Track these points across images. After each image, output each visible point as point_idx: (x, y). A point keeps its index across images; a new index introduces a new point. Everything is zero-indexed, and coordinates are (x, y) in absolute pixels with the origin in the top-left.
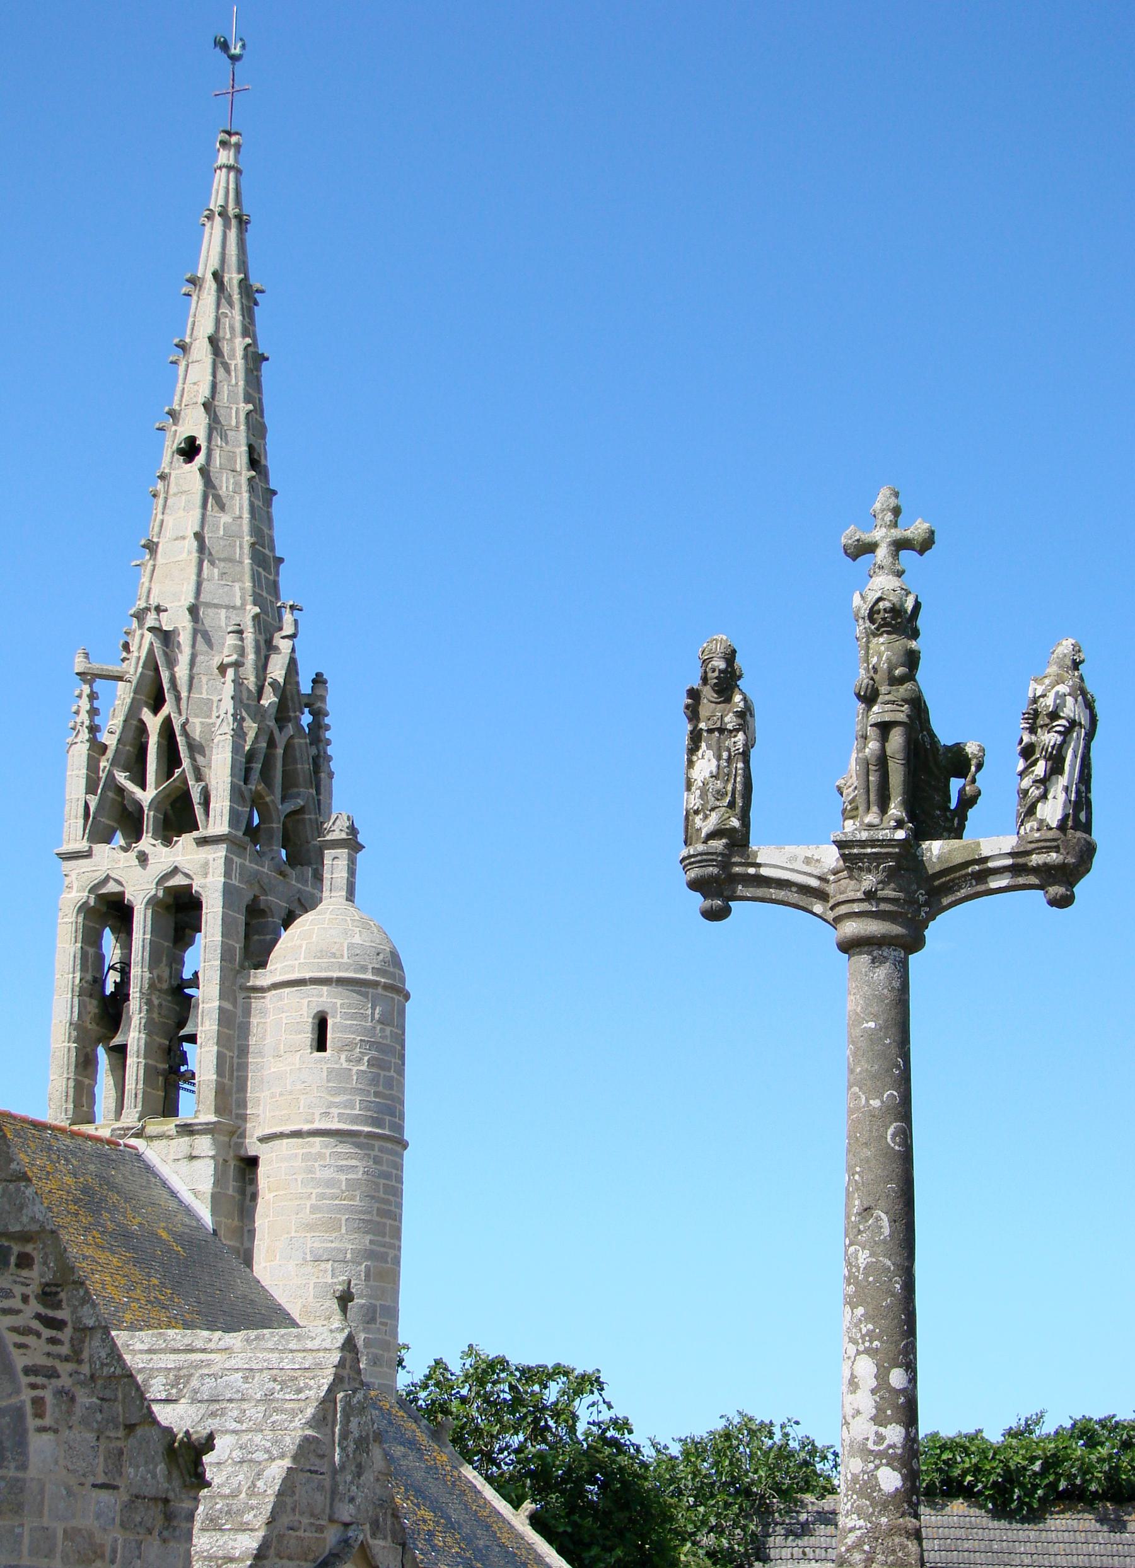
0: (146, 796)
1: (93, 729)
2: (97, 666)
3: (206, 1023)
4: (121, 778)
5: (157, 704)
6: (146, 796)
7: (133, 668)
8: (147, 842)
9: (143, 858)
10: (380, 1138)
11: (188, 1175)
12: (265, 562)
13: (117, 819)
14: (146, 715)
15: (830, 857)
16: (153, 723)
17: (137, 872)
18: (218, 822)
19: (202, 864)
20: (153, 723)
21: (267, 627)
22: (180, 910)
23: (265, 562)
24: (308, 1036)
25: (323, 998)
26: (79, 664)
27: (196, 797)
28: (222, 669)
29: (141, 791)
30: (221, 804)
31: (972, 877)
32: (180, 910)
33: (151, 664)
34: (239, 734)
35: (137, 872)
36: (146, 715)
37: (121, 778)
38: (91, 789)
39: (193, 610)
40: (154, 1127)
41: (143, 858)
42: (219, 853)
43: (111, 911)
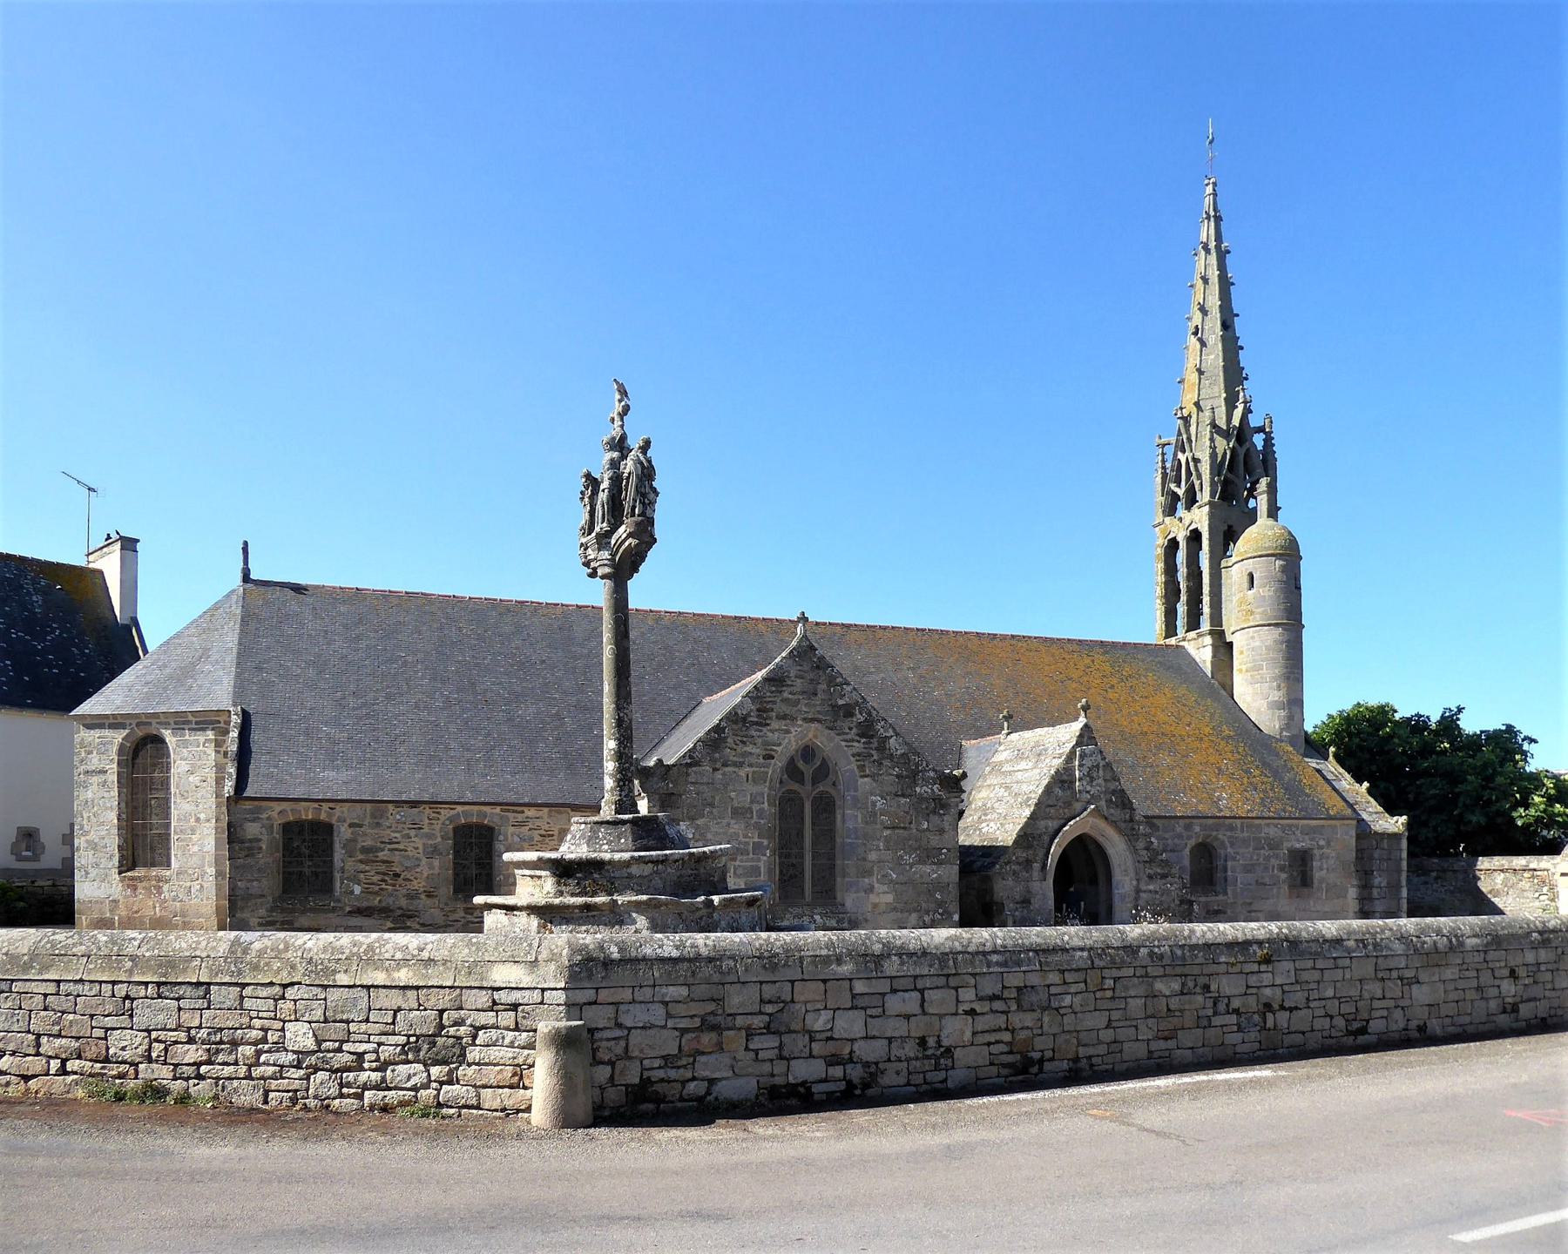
0: (1181, 492)
1: (1164, 468)
2: (1163, 441)
4: (1173, 486)
6: (1181, 492)
9: (1181, 519)
10: (1290, 620)
11: (1201, 651)
14: (1181, 456)
18: (1204, 496)
19: (1199, 518)
22: (1195, 536)
24: (1246, 585)
25: (1249, 565)
26: (1158, 441)
27: (1197, 488)
33: (1179, 434)
34: (1213, 455)
36: (1181, 456)
39: (1197, 404)
40: (1192, 634)
41: (1181, 519)
42: (1207, 508)
43: (1173, 545)
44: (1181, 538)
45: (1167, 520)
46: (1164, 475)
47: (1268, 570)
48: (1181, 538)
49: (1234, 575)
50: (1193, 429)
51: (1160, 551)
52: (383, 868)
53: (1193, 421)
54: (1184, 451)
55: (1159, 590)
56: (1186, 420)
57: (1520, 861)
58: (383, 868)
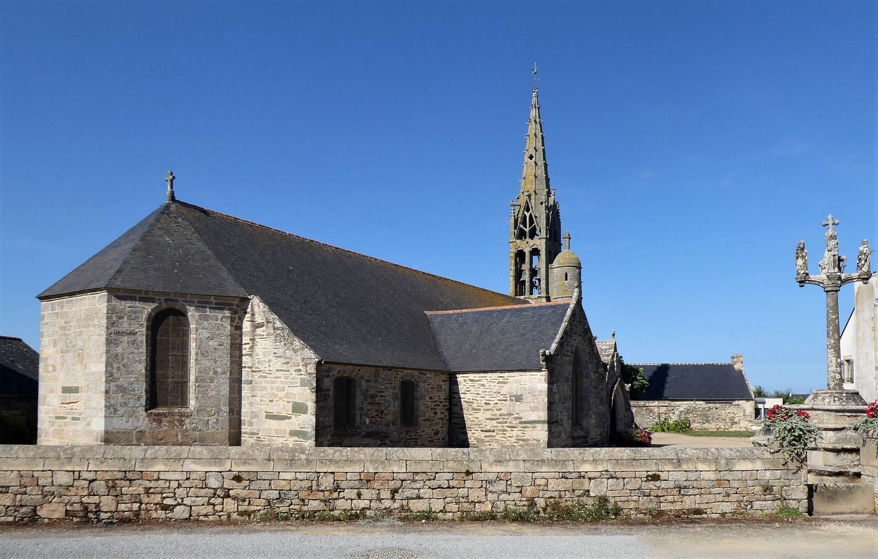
0: (527, 230)
3: (542, 274)
5: (528, 210)
6: (527, 230)
7: (523, 205)
8: (528, 239)
12: (547, 180)
13: (521, 235)
14: (526, 213)
15: (825, 277)
16: (528, 215)
17: (526, 246)
19: (540, 242)
20: (528, 215)
21: (549, 193)
22: (535, 252)
23: (547, 180)
25: (566, 269)
28: (542, 203)
29: (524, 229)
30: (544, 231)
31: (849, 280)
32: (535, 252)
33: (527, 202)
35: (526, 246)
37: (522, 226)
38: (515, 228)
42: (544, 241)
44: (527, 251)
45: (518, 241)
46: (516, 221)
47: (571, 273)
48: (527, 251)
49: (557, 271)
50: (533, 201)
51: (512, 255)
52: (377, 408)
53: (533, 197)
54: (528, 210)
55: (512, 273)
56: (529, 196)
57: (642, 403)
58: (377, 408)
